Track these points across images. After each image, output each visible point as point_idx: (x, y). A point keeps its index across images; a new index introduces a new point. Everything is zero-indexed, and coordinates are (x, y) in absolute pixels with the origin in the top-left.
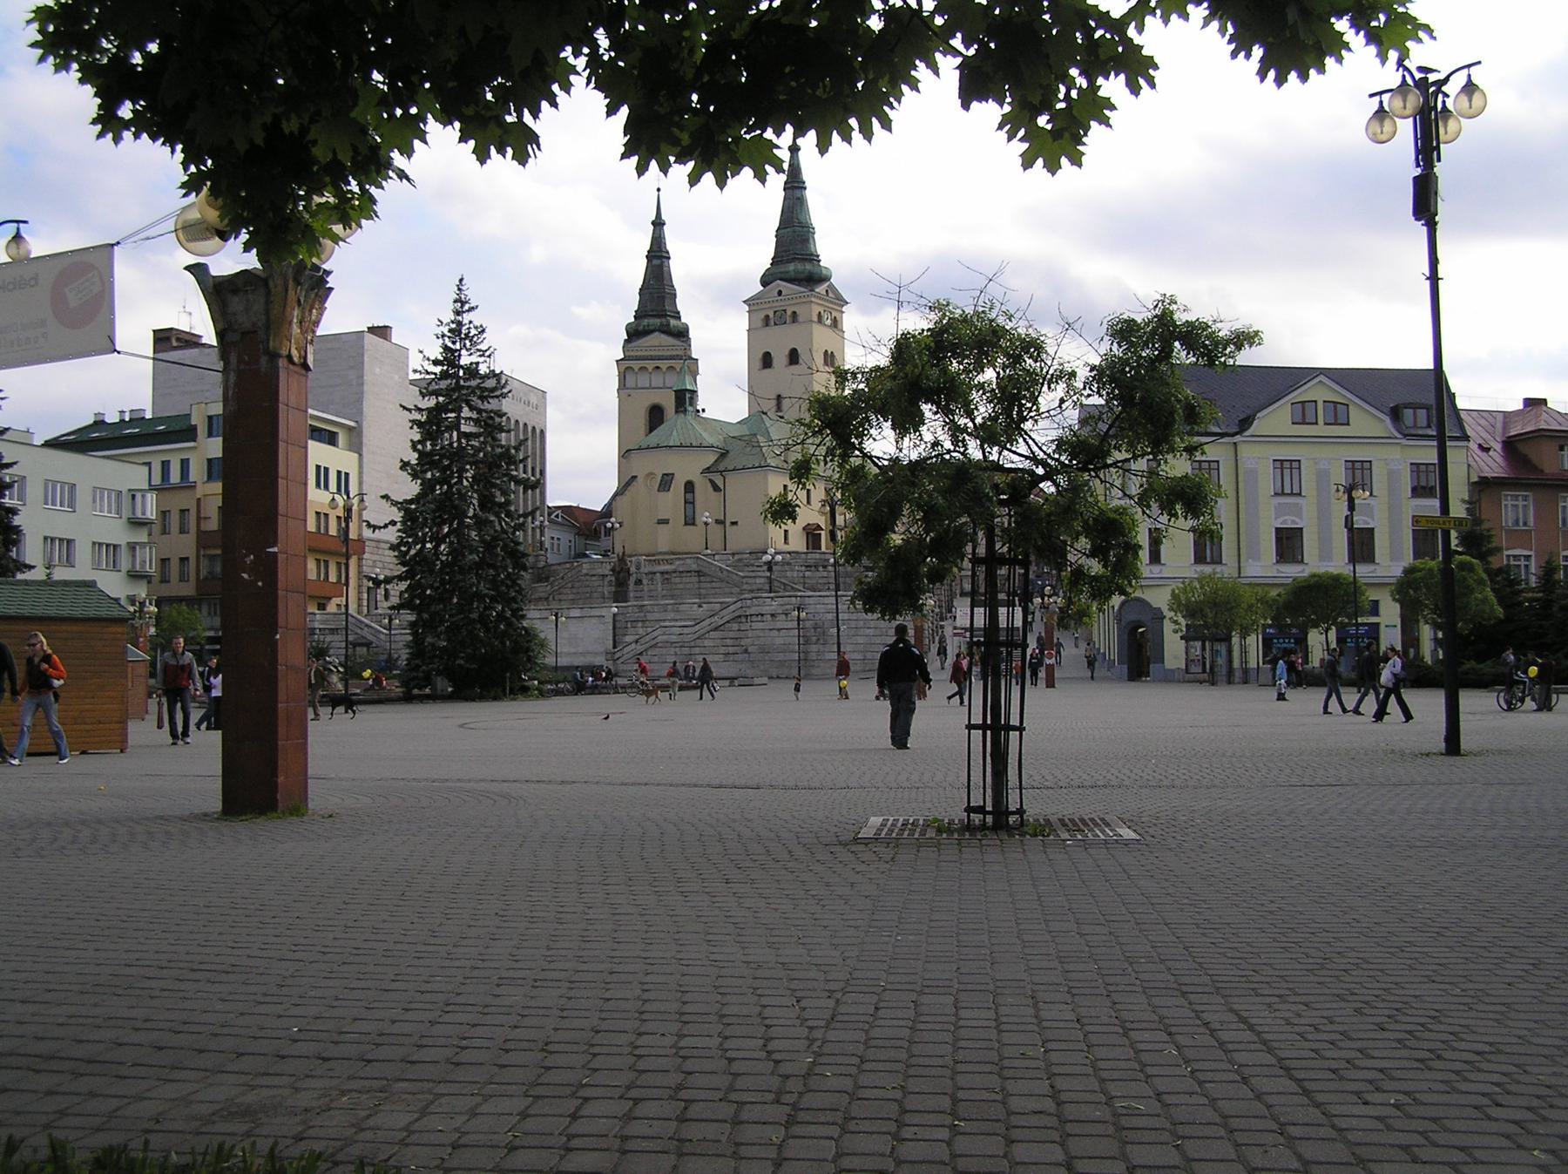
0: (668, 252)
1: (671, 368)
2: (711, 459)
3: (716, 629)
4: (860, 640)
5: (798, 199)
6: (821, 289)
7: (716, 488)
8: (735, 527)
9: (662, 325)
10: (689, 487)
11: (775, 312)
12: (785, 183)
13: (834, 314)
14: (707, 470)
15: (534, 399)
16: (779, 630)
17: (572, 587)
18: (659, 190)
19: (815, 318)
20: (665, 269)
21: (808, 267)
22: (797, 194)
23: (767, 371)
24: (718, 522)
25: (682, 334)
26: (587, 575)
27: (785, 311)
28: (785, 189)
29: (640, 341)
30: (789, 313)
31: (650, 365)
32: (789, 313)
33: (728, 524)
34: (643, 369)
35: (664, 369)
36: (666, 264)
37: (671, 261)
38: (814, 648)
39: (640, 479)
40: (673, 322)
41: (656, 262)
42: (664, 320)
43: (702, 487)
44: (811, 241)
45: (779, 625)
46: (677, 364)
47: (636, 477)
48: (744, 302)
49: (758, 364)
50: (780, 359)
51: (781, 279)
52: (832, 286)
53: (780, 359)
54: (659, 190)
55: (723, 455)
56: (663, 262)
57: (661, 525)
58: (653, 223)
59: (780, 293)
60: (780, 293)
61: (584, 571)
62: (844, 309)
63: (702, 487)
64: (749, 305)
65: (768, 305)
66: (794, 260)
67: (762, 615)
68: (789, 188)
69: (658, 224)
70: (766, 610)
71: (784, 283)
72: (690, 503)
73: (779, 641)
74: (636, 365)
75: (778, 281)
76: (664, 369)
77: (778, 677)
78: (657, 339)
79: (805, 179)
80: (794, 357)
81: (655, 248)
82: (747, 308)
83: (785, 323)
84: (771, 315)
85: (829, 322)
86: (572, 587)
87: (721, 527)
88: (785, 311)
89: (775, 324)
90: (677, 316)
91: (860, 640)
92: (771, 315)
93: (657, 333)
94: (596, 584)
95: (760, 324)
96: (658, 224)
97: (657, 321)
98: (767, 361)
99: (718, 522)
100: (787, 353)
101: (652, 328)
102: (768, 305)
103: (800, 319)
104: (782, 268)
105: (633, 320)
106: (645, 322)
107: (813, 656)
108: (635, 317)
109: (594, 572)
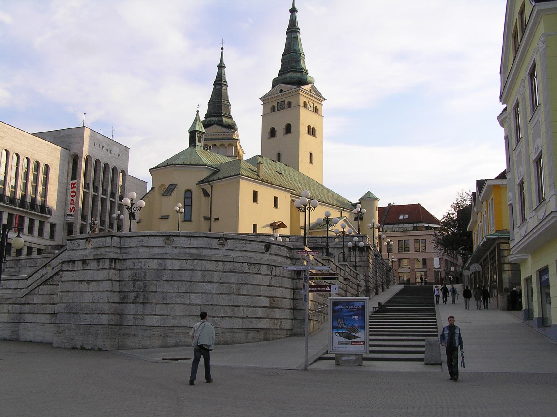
0: (226, 82)
2: (205, 174)
3: (45, 283)
4: (196, 299)
5: (295, 37)
6: (307, 87)
7: (206, 194)
8: (217, 222)
9: (218, 121)
10: (188, 195)
11: (278, 103)
12: (287, 30)
13: (316, 105)
14: (202, 182)
15: (116, 149)
16: (89, 282)
18: (222, 49)
19: (301, 104)
20: (223, 91)
21: (299, 75)
22: (294, 35)
23: (273, 139)
24: (205, 218)
25: (232, 127)
27: (284, 101)
28: (287, 33)
30: (286, 103)
32: (286, 103)
33: (213, 220)
36: (224, 88)
37: (228, 89)
38: (131, 309)
40: (225, 119)
41: (218, 87)
42: (220, 118)
43: (197, 194)
44: (302, 61)
45: (89, 275)
47: (154, 187)
48: (260, 99)
49: (268, 135)
50: (280, 131)
51: (282, 83)
52: (314, 89)
53: (280, 131)
54: (222, 49)
55: (215, 173)
57: (162, 220)
58: (218, 66)
59: (281, 91)
60: (281, 91)
62: (323, 103)
63: (197, 194)
64: (263, 101)
65: (273, 100)
66: (290, 72)
67: (74, 262)
69: (221, 67)
70: (79, 255)
72: (188, 205)
73: (87, 297)
77: (83, 348)
78: (215, 129)
79: (299, 27)
80: (288, 129)
81: (218, 79)
84: (276, 105)
85: (312, 109)
87: (207, 222)
88: (284, 101)
89: (278, 110)
90: (230, 117)
91: (196, 299)
92: (276, 105)
93: (215, 126)
95: (269, 111)
96: (221, 67)
97: (216, 119)
98: (273, 133)
99: (205, 218)
101: (212, 122)
102: (273, 100)
103: (293, 105)
104: (283, 77)
105: (204, 119)
106: (209, 119)
107: (129, 320)
108: (205, 118)
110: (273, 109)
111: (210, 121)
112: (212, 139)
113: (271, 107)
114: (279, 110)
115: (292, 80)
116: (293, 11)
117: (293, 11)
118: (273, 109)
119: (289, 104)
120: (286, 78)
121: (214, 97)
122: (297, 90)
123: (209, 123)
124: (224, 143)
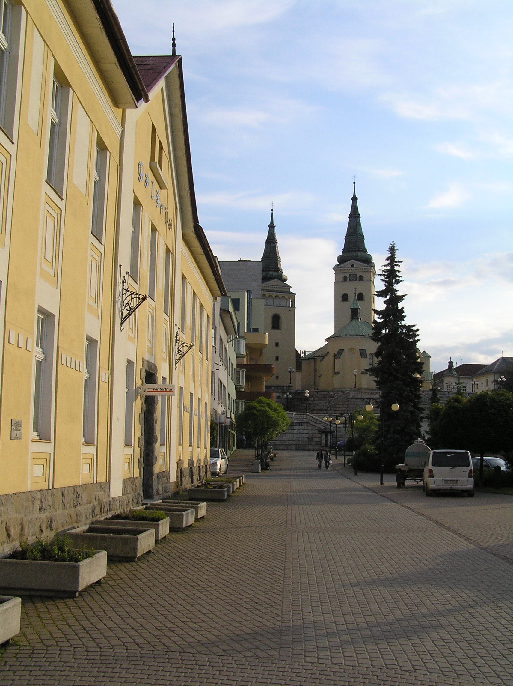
1: (283, 297)
11: (350, 275)
17: (343, 404)
18: (272, 210)
26: (352, 398)
27: (356, 275)
29: (270, 282)
30: (358, 276)
31: (276, 294)
32: (358, 276)
34: (270, 296)
35: (280, 297)
39: (346, 351)
46: (280, 295)
50: (351, 297)
51: (354, 259)
54: (272, 210)
56: (275, 245)
57: (363, 375)
59: (353, 266)
60: (353, 266)
61: (351, 396)
68: (352, 217)
71: (356, 261)
74: (267, 294)
75: (353, 260)
76: (280, 297)
79: (359, 213)
82: (334, 272)
83: (356, 280)
84: (348, 276)
86: (343, 404)
89: (350, 281)
92: (348, 276)
93: (276, 280)
94: (359, 403)
95: (342, 280)
98: (345, 298)
100: (342, 295)
101: (274, 276)
103: (364, 279)
109: (357, 397)
110: (345, 279)
111: (272, 275)
112: (274, 291)
113: (343, 277)
114: (351, 281)
115: (362, 259)
116: (354, 199)
117: (354, 199)
118: (345, 279)
119: (361, 278)
120: (358, 256)
121: (270, 254)
122: (369, 268)
123: (271, 276)
124: (285, 296)
